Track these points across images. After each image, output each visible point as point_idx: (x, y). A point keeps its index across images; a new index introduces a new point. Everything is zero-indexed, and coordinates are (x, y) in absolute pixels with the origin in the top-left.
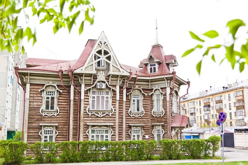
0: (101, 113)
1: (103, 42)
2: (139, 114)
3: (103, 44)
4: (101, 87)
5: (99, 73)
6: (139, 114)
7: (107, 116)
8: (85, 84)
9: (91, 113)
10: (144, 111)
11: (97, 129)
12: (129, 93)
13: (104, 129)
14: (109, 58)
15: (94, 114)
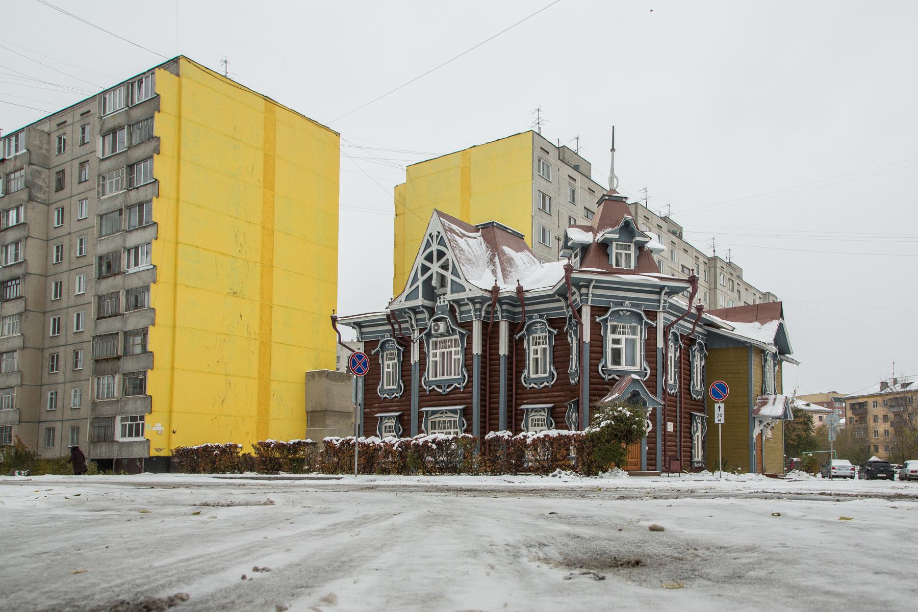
0: (446, 385)
2: (544, 380)
3: (435, 238)
5: (438, 301)
6: (542, 381)
8: (420, 329)
9: (430, 387)
15: (434, 388)
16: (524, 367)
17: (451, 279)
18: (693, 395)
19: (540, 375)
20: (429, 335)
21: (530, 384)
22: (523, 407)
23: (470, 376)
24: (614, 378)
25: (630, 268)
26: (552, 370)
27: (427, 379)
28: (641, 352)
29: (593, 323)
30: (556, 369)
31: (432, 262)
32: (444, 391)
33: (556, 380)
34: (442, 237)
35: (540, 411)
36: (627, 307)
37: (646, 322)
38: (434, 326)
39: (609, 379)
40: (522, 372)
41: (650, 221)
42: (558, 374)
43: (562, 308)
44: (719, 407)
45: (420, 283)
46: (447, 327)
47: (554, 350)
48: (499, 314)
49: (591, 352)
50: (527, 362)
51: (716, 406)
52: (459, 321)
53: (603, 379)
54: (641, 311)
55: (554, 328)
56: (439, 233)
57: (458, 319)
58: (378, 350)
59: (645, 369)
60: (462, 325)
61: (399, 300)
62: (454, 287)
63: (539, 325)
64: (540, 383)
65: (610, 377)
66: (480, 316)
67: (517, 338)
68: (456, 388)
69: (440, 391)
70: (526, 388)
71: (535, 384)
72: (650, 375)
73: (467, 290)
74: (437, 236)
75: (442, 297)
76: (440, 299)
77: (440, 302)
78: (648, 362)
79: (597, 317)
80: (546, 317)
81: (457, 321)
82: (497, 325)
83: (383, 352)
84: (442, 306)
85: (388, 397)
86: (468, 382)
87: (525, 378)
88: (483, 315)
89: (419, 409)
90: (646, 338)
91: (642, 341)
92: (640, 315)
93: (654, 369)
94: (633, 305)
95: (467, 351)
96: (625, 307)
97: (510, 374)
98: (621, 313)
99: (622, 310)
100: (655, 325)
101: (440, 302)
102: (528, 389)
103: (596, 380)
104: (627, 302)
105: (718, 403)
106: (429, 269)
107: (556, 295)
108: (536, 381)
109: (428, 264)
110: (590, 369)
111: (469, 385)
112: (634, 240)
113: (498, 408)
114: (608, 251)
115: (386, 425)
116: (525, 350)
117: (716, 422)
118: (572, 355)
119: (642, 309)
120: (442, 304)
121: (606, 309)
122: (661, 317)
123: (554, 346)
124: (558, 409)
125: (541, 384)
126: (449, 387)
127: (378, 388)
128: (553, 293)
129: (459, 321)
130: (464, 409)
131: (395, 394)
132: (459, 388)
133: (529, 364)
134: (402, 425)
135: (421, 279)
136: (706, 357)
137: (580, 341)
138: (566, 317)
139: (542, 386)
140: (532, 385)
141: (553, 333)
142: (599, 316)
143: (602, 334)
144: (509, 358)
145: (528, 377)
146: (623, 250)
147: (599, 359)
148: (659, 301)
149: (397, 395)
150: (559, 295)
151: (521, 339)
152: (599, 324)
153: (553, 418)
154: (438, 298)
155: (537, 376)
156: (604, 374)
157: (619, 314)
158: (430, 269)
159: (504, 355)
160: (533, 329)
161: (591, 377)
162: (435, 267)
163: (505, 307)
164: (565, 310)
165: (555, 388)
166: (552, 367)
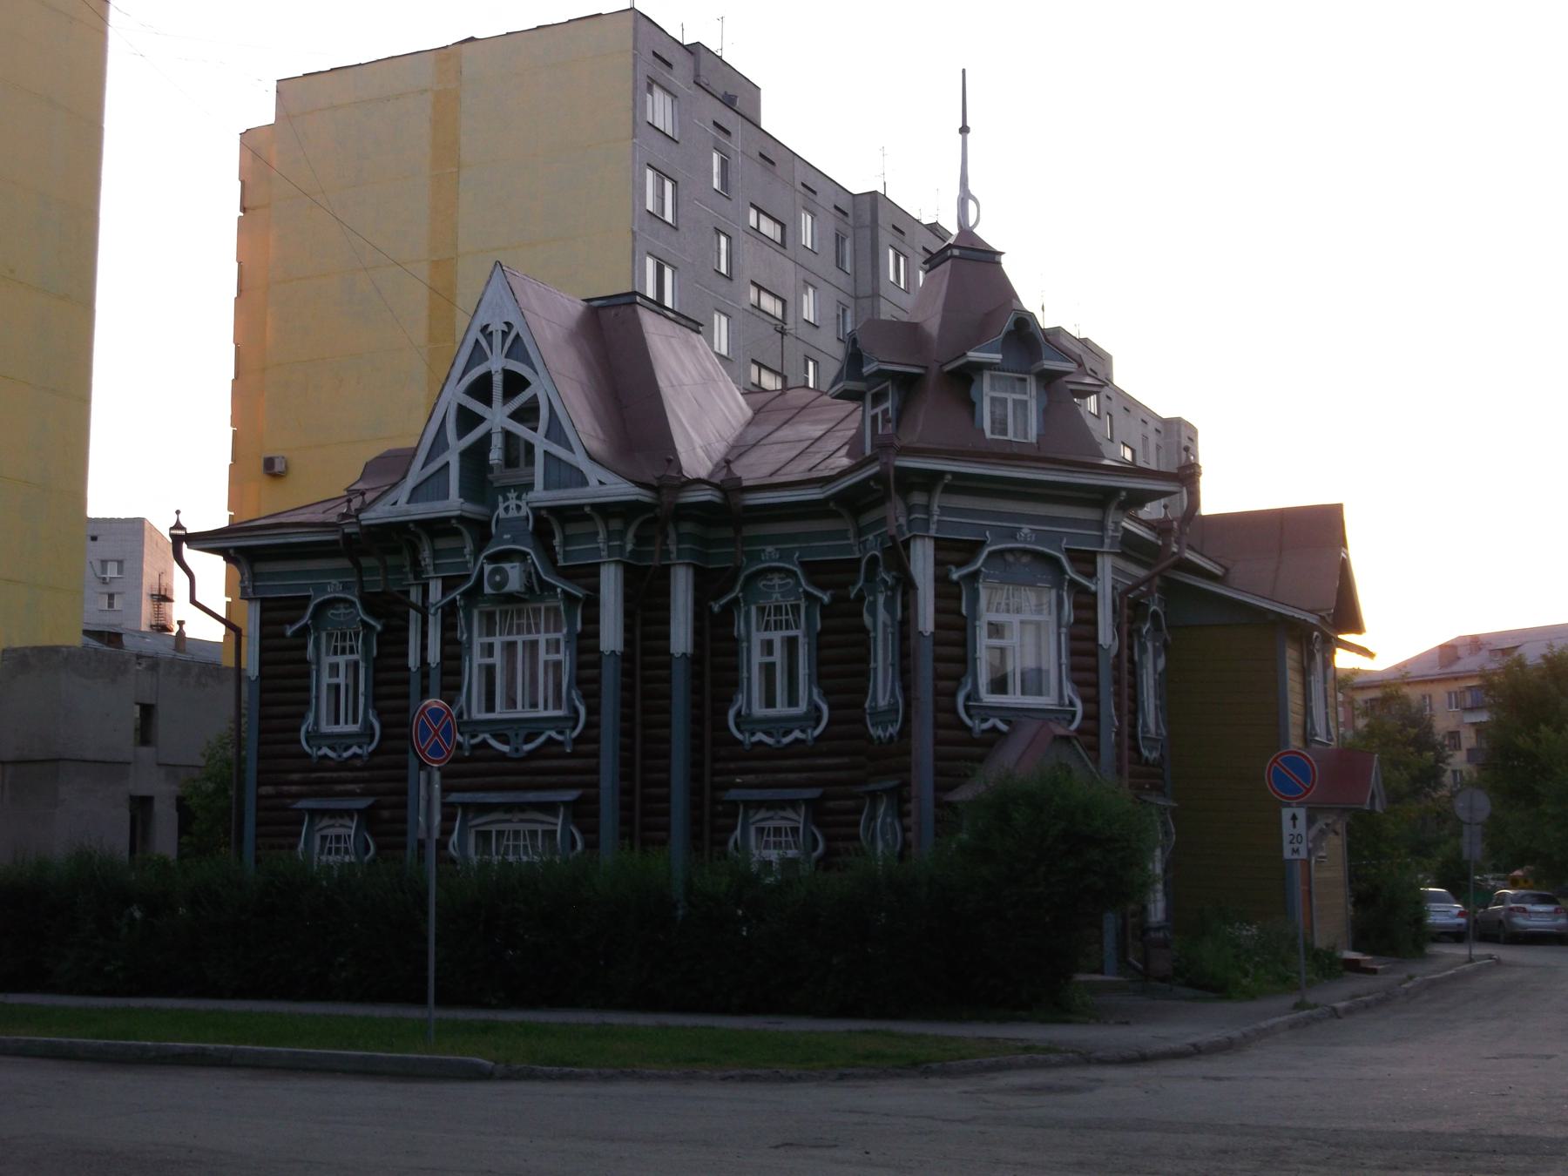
0: (523, 733)
1: (497, 327)
3: (497, 339)
4: (499, 586)
7: (555, 749)
8: (444, 578)
9: (474, 736)
10: (825, 708)
11: (501, 827)
12: (723, 601)
13: (540, 828)
14: (527, 414)
16: (735, 684)
17: (546, 452)
18: (1143, 750)
19: (781, 709)
20: (474, 594)
21: (753, 734)
22: (733, 794)
24: (994, 729)
25: (1026, 438)
26: (816, 697)
27: (465, 717)
28: (1060, 657)
29: (941, 580)
31: (488, 401)
33: (828, 725)
34: (518, 335)
35: (783, 808)
36: (1025, 541)
37: (1072, 582)
38: (494, 572)
39: (984, 731)
40: (730, 701)
41: (907, 238)
42: (831, 708)
43: (842, 534)
44: (1294, 818)
45: (453, 458)
46: (529, 576)
47: (821, 643)
48: (673, 548)
49: (937, 659)
50: (745, 674)
51: (1286, 813)
52: (561, 563)
53: (969, 729)
54: (1060, 550)
55: (823, 588)
56: (508, 324)
57: (560, 557)
58: (306, 625)
59: (1072, 704)
60: (567, 574)
61: (391, 498)
65: (986, 726)
66: (622, 548)
67: (716, 608)
69: (505, 748)
70: (740, 743)
72: (1085, 717)
73: (593, 481)
74: (505, 334)
75: (512, 495)
76: (506, 499)
77: (507, 509)
78: (1077, 683)
79: (953, 568)
80: (798, 558)
81: (554, 562)
82: (665, 573)
83: (317, 629)
85: (331, 754)
86: (588, 725)
87: (738, 714)
88: (629, 547)
90: (1072, 620)
91: (1064, 630)
92: (1055, 562)
93: (1091, 701)
94: (1040, 537)
95: (586, 641)
96: (1021, 542)
98: (1010, 558)
99: (1011, 551)
100: (1093, 588)
101: (507, 509)
104: (1026, 529)
105: (1289, 805)
106: (481, 420)
108: (769, 725)
109: (477, 407)
110: (936, 703)
111: (590, 735)
112: (1036, 367)
113: (666, 799)
114: (974, 393)
115: (325, 832)
116: (736, 641)
117: (1287, 854)
118: (875, 661)
119: (1063, 546)
120: (513, 513)
121: (974, 547)
122: (1105, 565)
123: (820, 634)
124: (831, 804)
125: (787, 733)
126: (529, 739)
127: (303, 729)
128: (821, 496)
129: (561, 563)
131: (355, 749)
132: (561, 743)
133: (749, 679)
134: (373, 835)
135: (456, 446)
136: (1166, 646)
137: (905, 628)
138: (859, 560)
140: (760, 736)
141: (819, 600)
142: (959, 565)
143: (964, 611)
144: (695, 660)
146: (1006, 391)
147: (958, 679)
148: (1101, 526)
149: (359, 751)
151: (729, 609)
152: (957, 584)
153: (818, 826)
154: (500, 499)
155: (771, 712)
156: (970, 717)
157: (1005, 560)
158: (481, 419)
159: (684, 654)
161: (937, 725)
162: (497, 417)
163: (687, 527)
164: (852, 541)
166: (815, 691)
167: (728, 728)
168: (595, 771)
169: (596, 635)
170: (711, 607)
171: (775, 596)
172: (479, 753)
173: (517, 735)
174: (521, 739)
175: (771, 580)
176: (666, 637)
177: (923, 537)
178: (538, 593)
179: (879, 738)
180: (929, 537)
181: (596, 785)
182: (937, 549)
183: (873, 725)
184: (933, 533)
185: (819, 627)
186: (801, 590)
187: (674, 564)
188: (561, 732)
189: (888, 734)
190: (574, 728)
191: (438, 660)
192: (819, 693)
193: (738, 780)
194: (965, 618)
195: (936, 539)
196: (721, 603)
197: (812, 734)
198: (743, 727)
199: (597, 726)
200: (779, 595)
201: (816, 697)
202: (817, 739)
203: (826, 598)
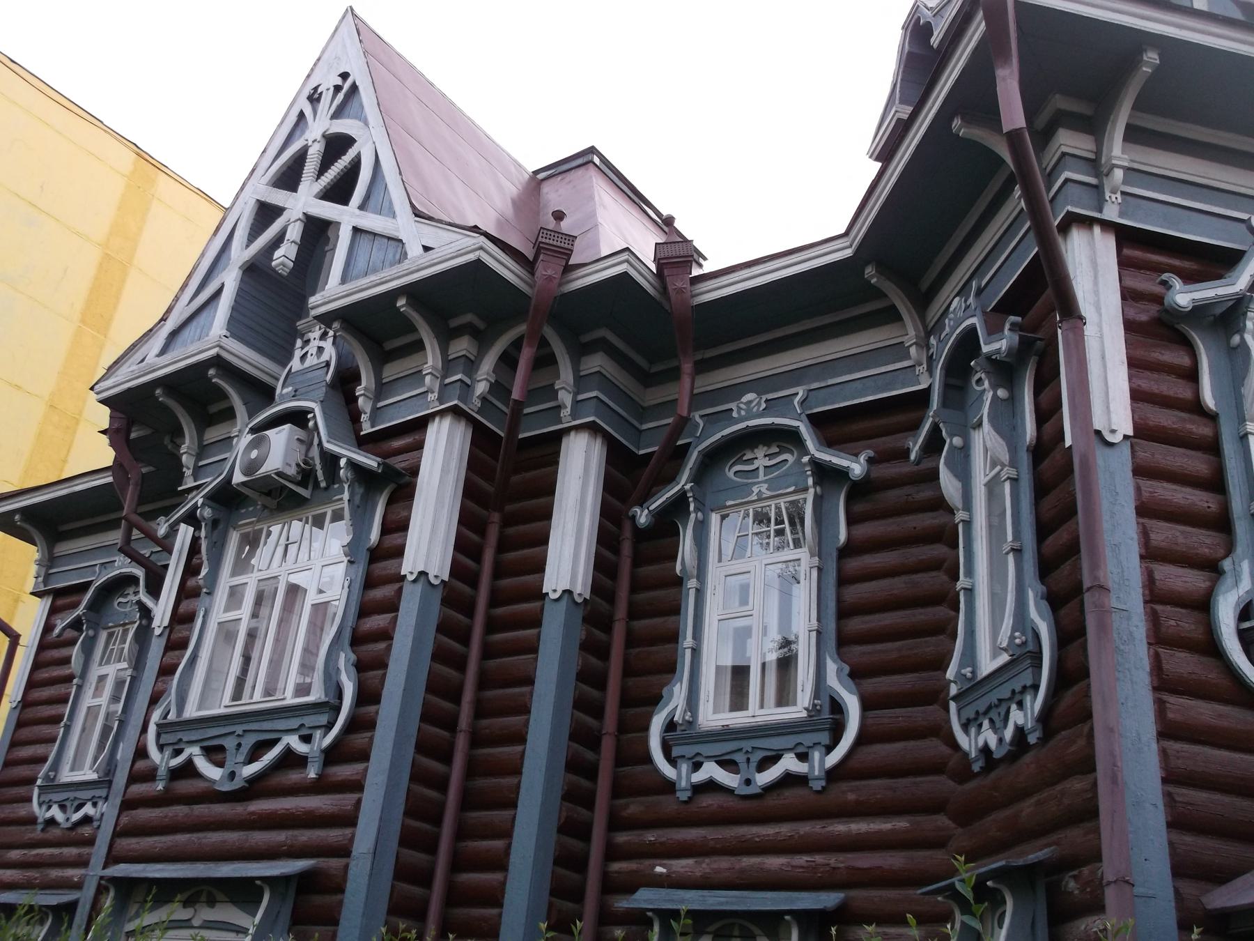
2: (775, 743)
5: (298, 354)
6: (775, 743)
7: (294, 777)
9: (178, 752)
16: (670, 668)
21: (697, 766)
22: (645, 898)
23: (368, 696)
26: (832, 680)
30: (856, 675)
32: (232, 775)
33: (860, 740)
34: (354, 88)
40: (655, 700)
42: (867, 705)
45: (230, 279)
48: (566, 398)
50: (688, 641)
62: (360, 263)
63: (760, 452)
64: (756, 757)
66: (467, 388)
67: (643, 517)
68: (291, 760)
70: (669, 787)
71: (727, 764)
73: (414, 250)
79: (1177, 283)
80: (802, 403)
83: (96, 626)
84: (312, 369)
87: (671, 726)
88: (481, 388)
89: (104, 868)
97: (588, 706)
101: (303, 358)
102: (683, 796)
103: (1205, 712)
107: (869, 271)
118: (970, 573)
123: (845, 552)
125: (764, 764)
128: (848, 253)
129: (367, 429)
130: (305, 883)
135: (240, 254)
139: (765, 778)
140: (711, 771)
141: (841, 474)
145: (691, 724)
150: (884, 268)
155: (738, 719)
159: (567, 592)
160: (731, 474)
163: (596, 363)
165: (849, 792)
166: (831, 667)
167: (648, 759)
168: (349, 820)
169: (399, 552)
170: (634, 517)
171: (755, 489)
172: (185, 786)
173: (239, 745)
174: (241, 758)
175: (751, 461)
176: (539, 567)
177: (1087, 222)
178: (323, 485)
179: (986, 750)
180: (1107, 225)
181: (344, 851)
182: (1124, 264)
183: (965, 727)
184: (1111, 213)
185: (843, 537)
186: (806, 459)
187: (567, 431)
188: (306, 739)
189: (1008, 733)
190: (329, 726)
191: (166, 623)
192: (839, 671)
193: (659, 869)
194: (1212, 417)
195: (1126, 237)
196: (652, 508)
197: (822, 762)
198: (676, 752)
199: (370, 725)
200: (764, 487)
201: (832, 680)
202: (833, 775)
203: (857, 468)
